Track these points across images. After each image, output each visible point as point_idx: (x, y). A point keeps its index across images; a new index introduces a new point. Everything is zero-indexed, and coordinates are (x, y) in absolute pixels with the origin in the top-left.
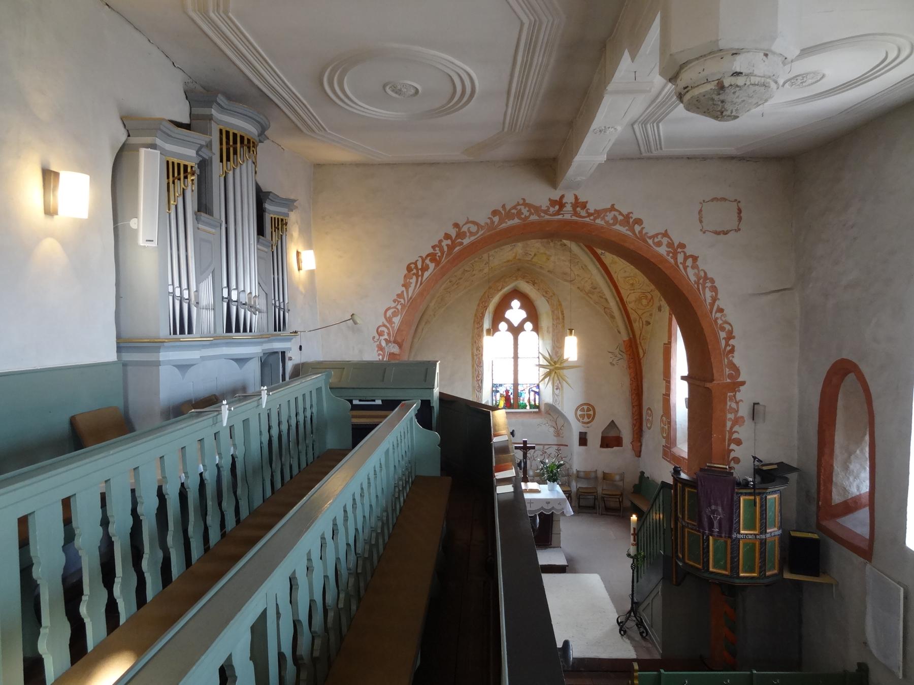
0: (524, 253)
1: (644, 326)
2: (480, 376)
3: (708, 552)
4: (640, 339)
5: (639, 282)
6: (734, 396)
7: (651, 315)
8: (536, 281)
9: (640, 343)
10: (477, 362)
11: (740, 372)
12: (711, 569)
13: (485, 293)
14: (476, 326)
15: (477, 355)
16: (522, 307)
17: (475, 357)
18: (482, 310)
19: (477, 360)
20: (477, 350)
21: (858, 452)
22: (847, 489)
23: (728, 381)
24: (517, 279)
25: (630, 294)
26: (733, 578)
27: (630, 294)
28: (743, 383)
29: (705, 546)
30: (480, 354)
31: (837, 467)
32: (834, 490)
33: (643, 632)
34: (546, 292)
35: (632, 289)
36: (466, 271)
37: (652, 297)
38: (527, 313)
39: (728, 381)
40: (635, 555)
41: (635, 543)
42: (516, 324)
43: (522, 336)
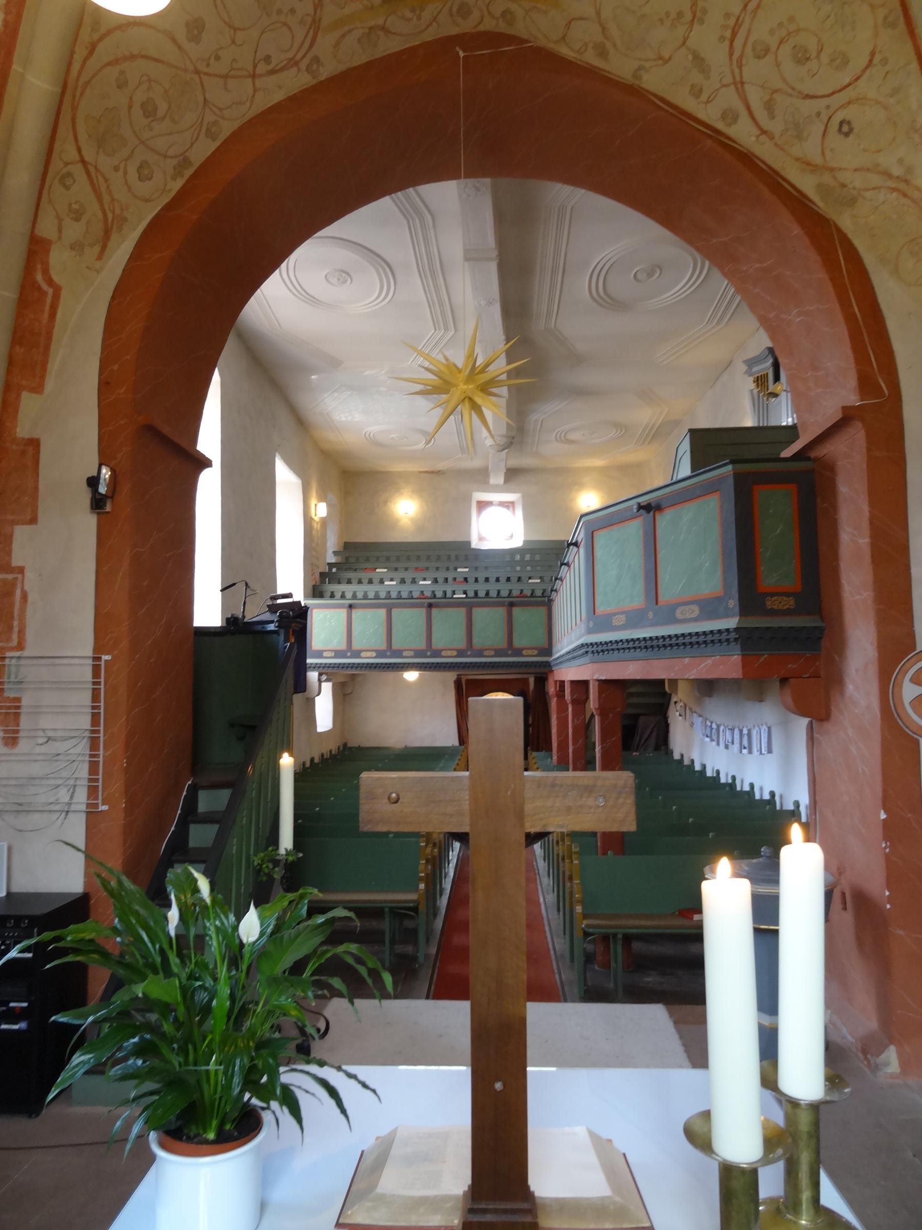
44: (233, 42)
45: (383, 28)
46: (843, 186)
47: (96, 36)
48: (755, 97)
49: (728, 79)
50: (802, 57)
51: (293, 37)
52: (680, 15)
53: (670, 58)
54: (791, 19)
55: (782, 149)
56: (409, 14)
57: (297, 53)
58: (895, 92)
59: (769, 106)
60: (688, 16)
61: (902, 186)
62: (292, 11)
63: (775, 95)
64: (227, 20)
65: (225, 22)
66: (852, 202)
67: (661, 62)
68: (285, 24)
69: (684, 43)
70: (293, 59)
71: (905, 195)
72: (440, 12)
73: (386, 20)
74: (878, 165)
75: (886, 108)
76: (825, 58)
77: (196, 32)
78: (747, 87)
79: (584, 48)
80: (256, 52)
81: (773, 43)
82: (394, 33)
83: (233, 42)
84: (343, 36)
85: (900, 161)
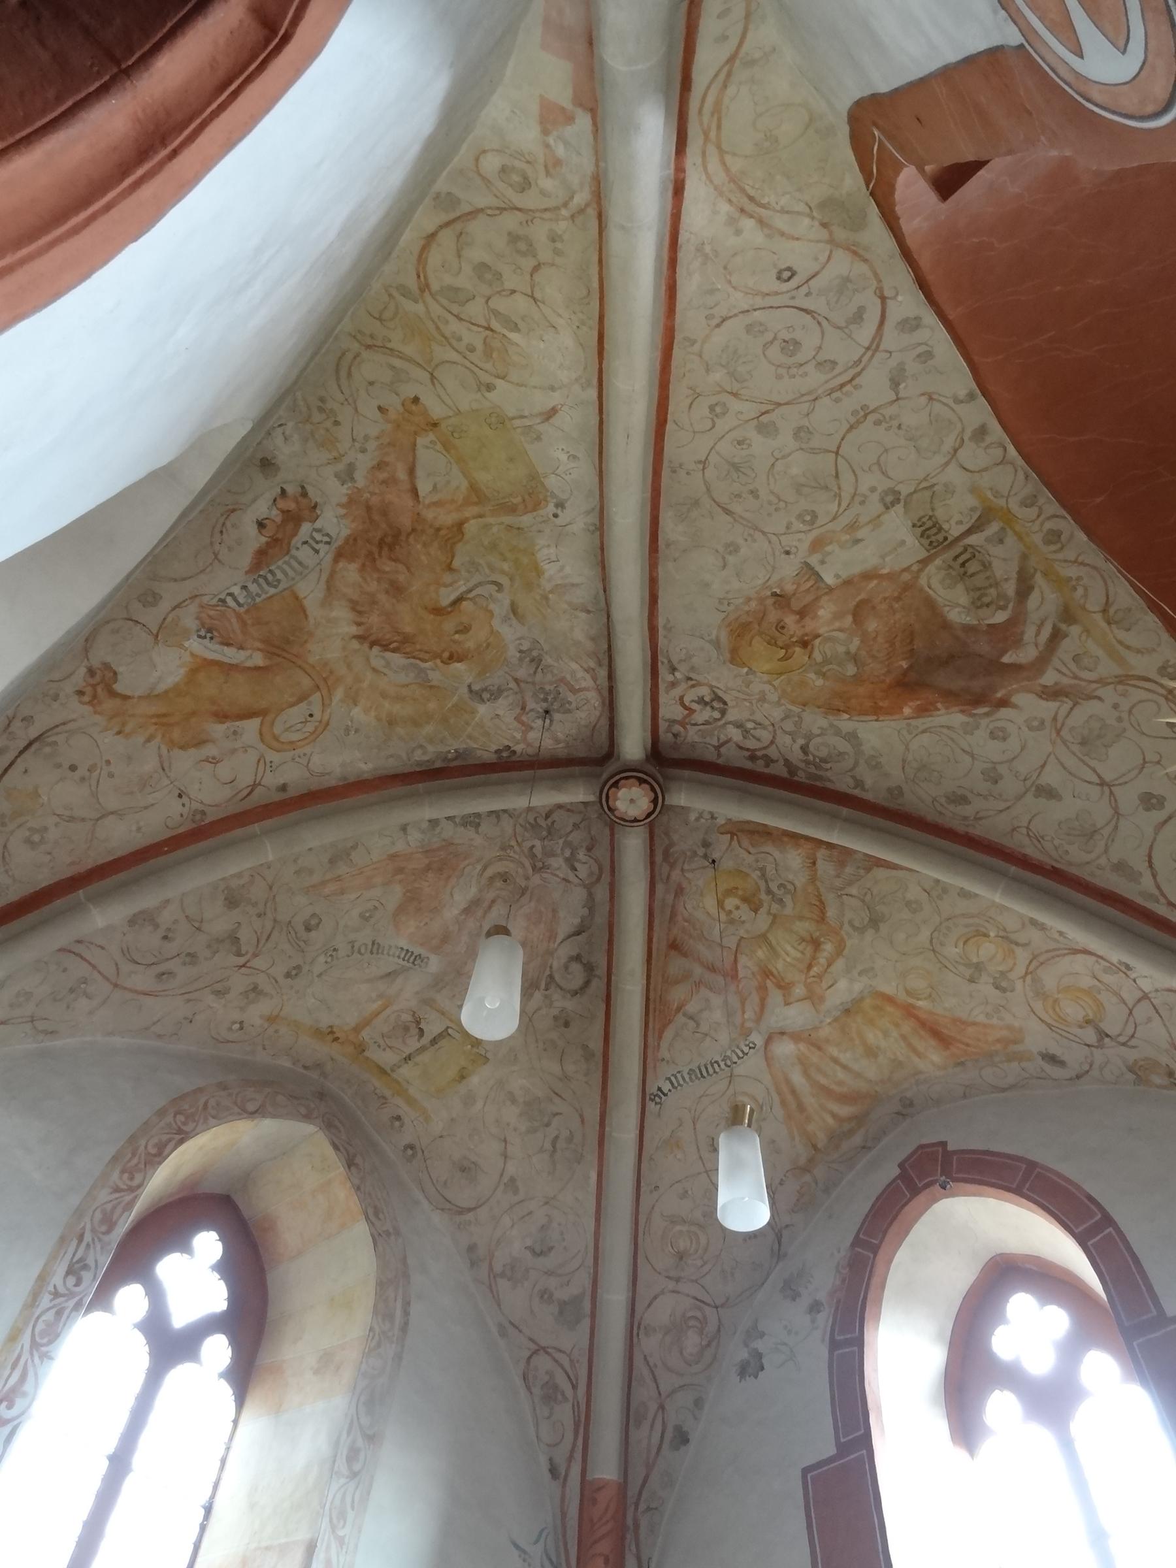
0: (407, 1017)
1: (666, 1446)
2: (19, 1404)
4: (637, 1505)
5: (706, 1250)
7: (698, 1403)
8: (358, 1160)
9: (637, 1525)
10: (41, 1326)
13: (200, 1090)
14: (115, 1176)
15: (56, 1294)
16: (227, 1268)
17: (45, 1301)
18: (165, 1138)
19: (49, 1316)
20: (69, 1272)
24: (307, 1117)
25: (662, 1292)
27: (662, 1292)
30: (70, 1295)
34: (376, 1214)
35: (672, 1274)
36: (235, 940)
37: (719, 1330)
38: (233, 1299)
42: (181, 1317)
43: (180, 1375)
44: (1158, 762)
45: (1104, 611)
46: (824, 225)
47: (1162, 900)
48: (865, 333)
49: (880, 356)
50: (791, 346)
51: (1141, 702)
52: (878, 423)
53: (923, 394)
54: (779, 377)
55: (876, 275)
56: (1080, 591)
57: (1158, 694)
58: (712, 292)
59: (858, 317)
60: (871, 418)
61: (750, 207)
62: (1116, 706)
63: (844, 324)
64: (1136, 771)
65: (1140, 773)
66: (827, 204)
67: (935, 397)
68: (1130, 712)
69: (898, 399)
70: (1167, 699)
71: (751, 199)
72: (1066, 561)
73: (1094, 612)
74: (769, 236)
75: (730, 282)
76: (769, 336)
77: (1154, 801)
78: (866, 344)
79: (993, 445)
80: (1167, 738)
81: (810, 368)
82: (1108, 598)
83: (1158, 762)
84: (1128, 648)
85: (738, 232)
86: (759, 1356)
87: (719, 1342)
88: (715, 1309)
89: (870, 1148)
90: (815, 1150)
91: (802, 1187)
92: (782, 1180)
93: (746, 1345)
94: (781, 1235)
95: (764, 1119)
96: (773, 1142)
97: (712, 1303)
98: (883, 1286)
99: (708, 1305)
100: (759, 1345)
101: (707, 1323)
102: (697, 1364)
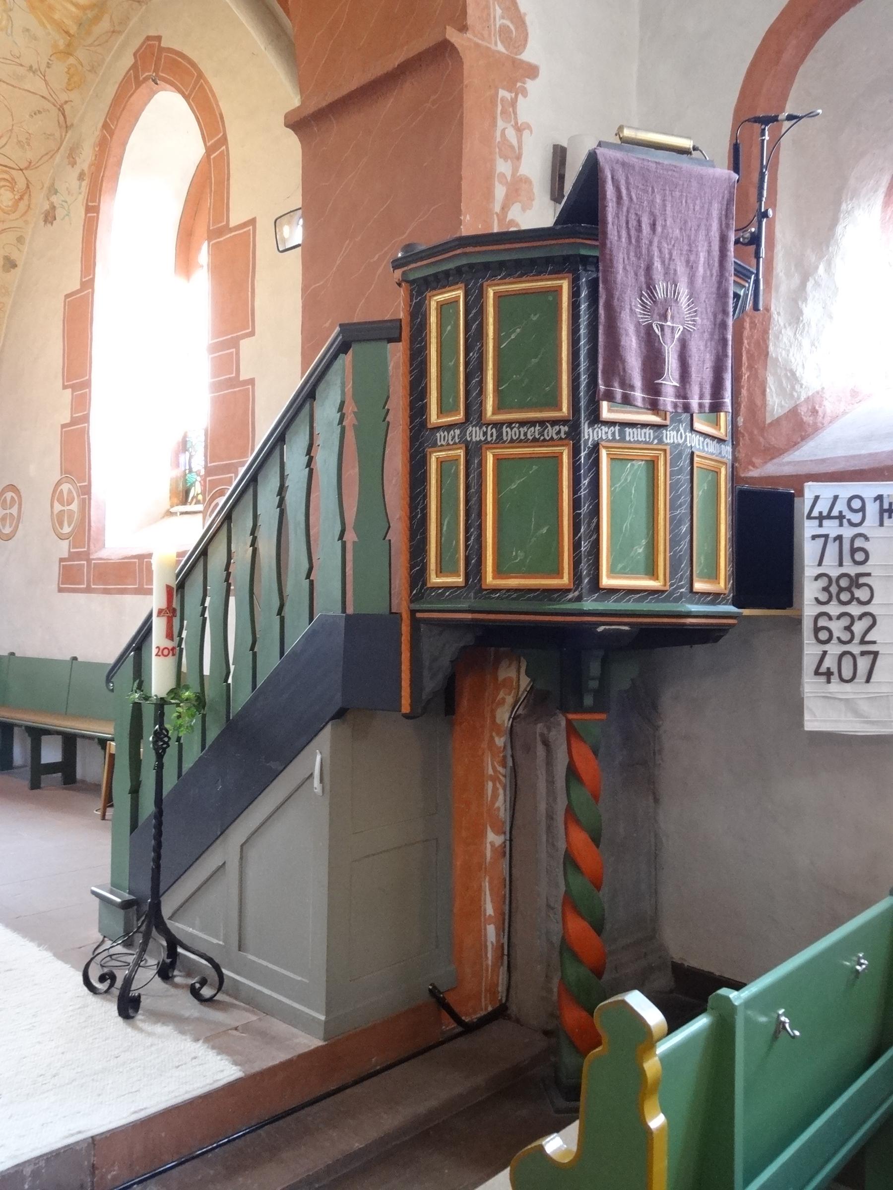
3: (596, 511)
6: (514, 103)
7: (20, 240)
11: (527, 34)
12: (606, 581)
21: (821, 269)
22: (798, 374)
23: (500, 48)
26: (677, 600)
28: (532, 71)
29: (583, 493)
31: (779, 314)
32: (771, 381)
33: (203, 982)
37: (28, 187)
39: (500, 48)
40: (172, 691)
41: (169, 644)
86: (54, 208)
87: (30, 195)
88: (20, 171)
89: (120, 32)
90: (69, 36)
91: (69, 69)
92: (48, 63)
93: (48, 199)
94: (63, 109)
95: (11, 10)
96: (28, 30)
97: (18, 168)
98: (119, 163)
99: (14, 169)
100: (54, 199)
101: (15, 183)
102: (14, 213)
